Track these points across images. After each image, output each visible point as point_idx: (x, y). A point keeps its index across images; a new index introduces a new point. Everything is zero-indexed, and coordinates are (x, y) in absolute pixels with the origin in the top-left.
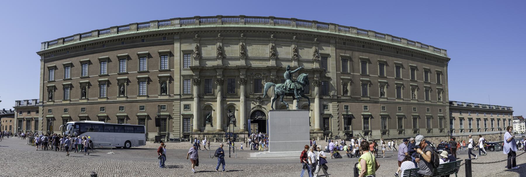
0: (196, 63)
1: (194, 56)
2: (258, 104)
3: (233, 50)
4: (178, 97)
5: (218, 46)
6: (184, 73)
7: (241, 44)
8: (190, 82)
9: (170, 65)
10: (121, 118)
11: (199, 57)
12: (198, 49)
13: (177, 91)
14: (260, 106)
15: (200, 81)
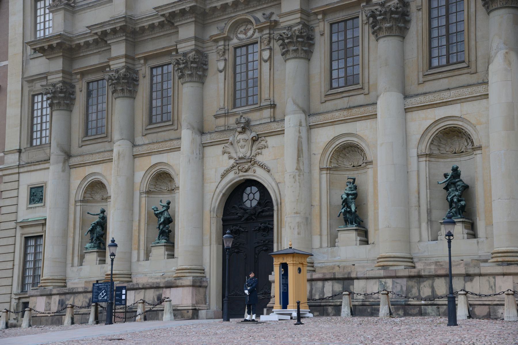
2: (243, 151)
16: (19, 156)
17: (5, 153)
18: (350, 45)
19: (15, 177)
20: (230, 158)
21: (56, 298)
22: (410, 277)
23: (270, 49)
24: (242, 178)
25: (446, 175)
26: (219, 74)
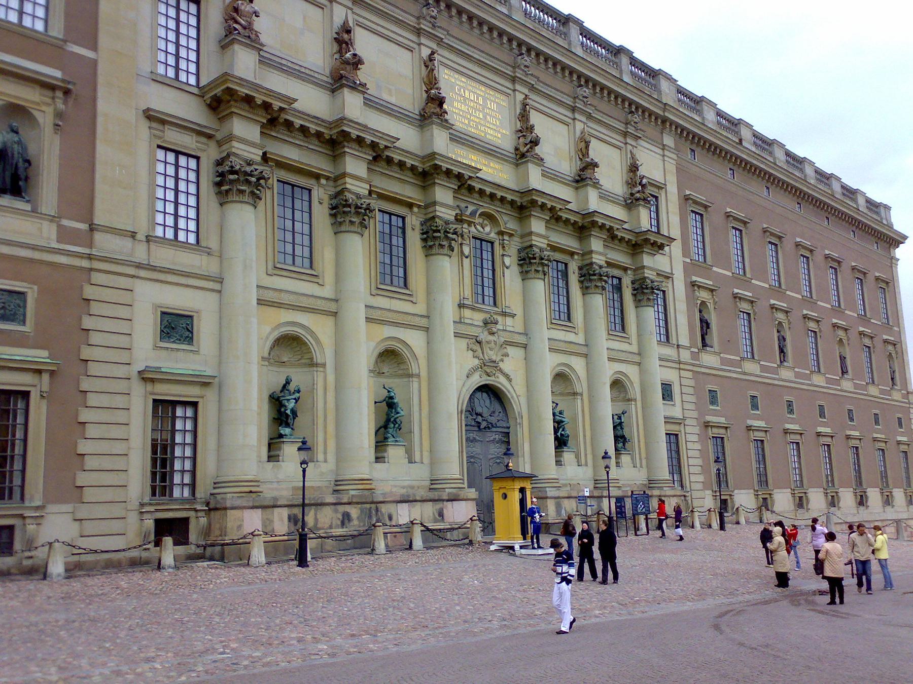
19: (123, 282)
21: (285, 512)
24: (487, 382)
26: (464, 259)
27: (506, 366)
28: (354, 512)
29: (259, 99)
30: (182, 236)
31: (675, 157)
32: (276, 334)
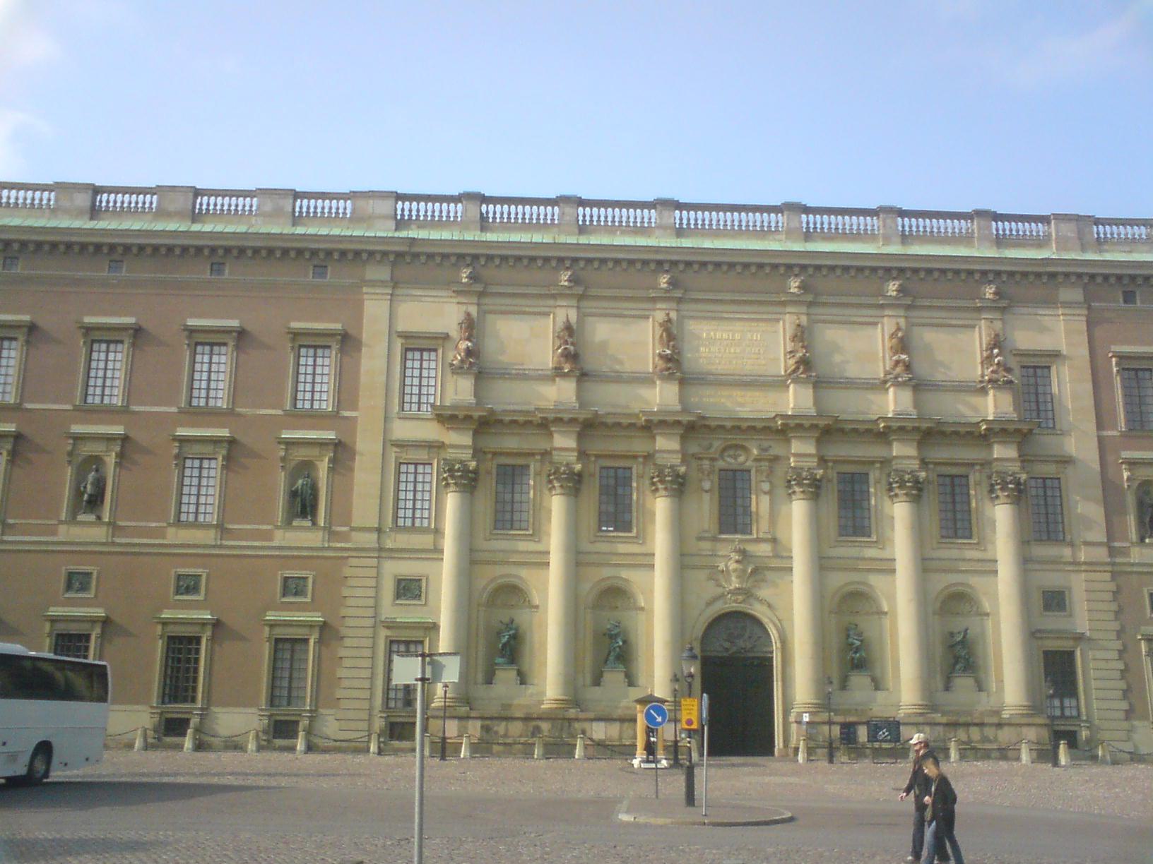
0: (461, 391)
1: (456, 357)
3: (630, 340)
4: (370, 539)
5: (561, 320)
6: (404, 430)
7: (660, 316)
8: (431, 475)
9: (339, 391)
10: (74, 629)
11: (476, 364)
12: (471, 327)
13: (364, 509)
14: (747, 594)
15: (476, 472)
16: (379, 538)
17: (353, 529)
18: (857, 497)
20: (720, 585)
22: (947, 725)
23: (771, 482)
25: (952, 634)
27: (764, 593)
28: (545, 726)
29: (461, 414)
30: (418, 523)
31: (1085, 312)
32: (493, 585)
